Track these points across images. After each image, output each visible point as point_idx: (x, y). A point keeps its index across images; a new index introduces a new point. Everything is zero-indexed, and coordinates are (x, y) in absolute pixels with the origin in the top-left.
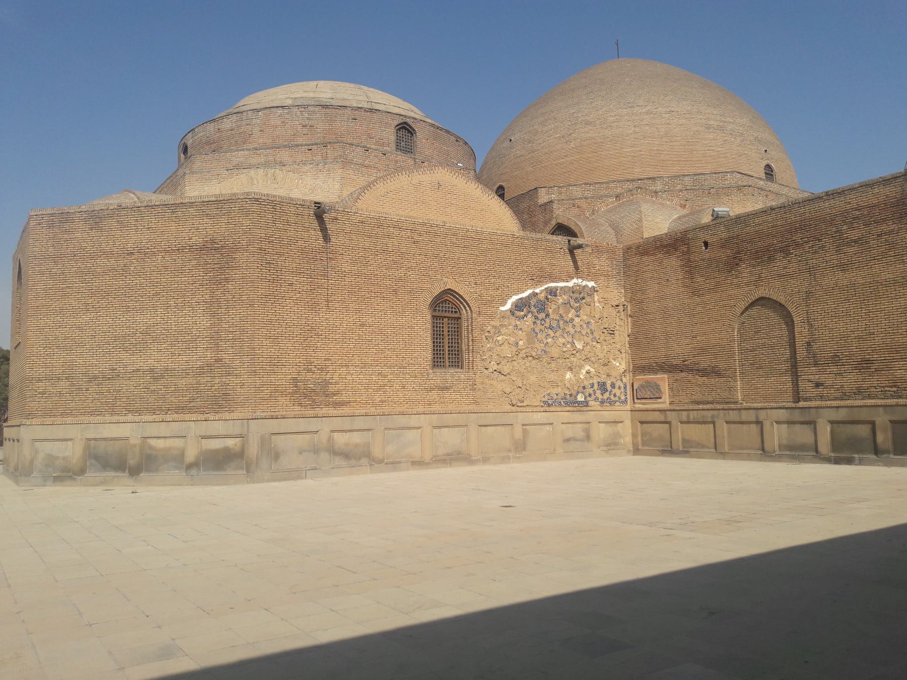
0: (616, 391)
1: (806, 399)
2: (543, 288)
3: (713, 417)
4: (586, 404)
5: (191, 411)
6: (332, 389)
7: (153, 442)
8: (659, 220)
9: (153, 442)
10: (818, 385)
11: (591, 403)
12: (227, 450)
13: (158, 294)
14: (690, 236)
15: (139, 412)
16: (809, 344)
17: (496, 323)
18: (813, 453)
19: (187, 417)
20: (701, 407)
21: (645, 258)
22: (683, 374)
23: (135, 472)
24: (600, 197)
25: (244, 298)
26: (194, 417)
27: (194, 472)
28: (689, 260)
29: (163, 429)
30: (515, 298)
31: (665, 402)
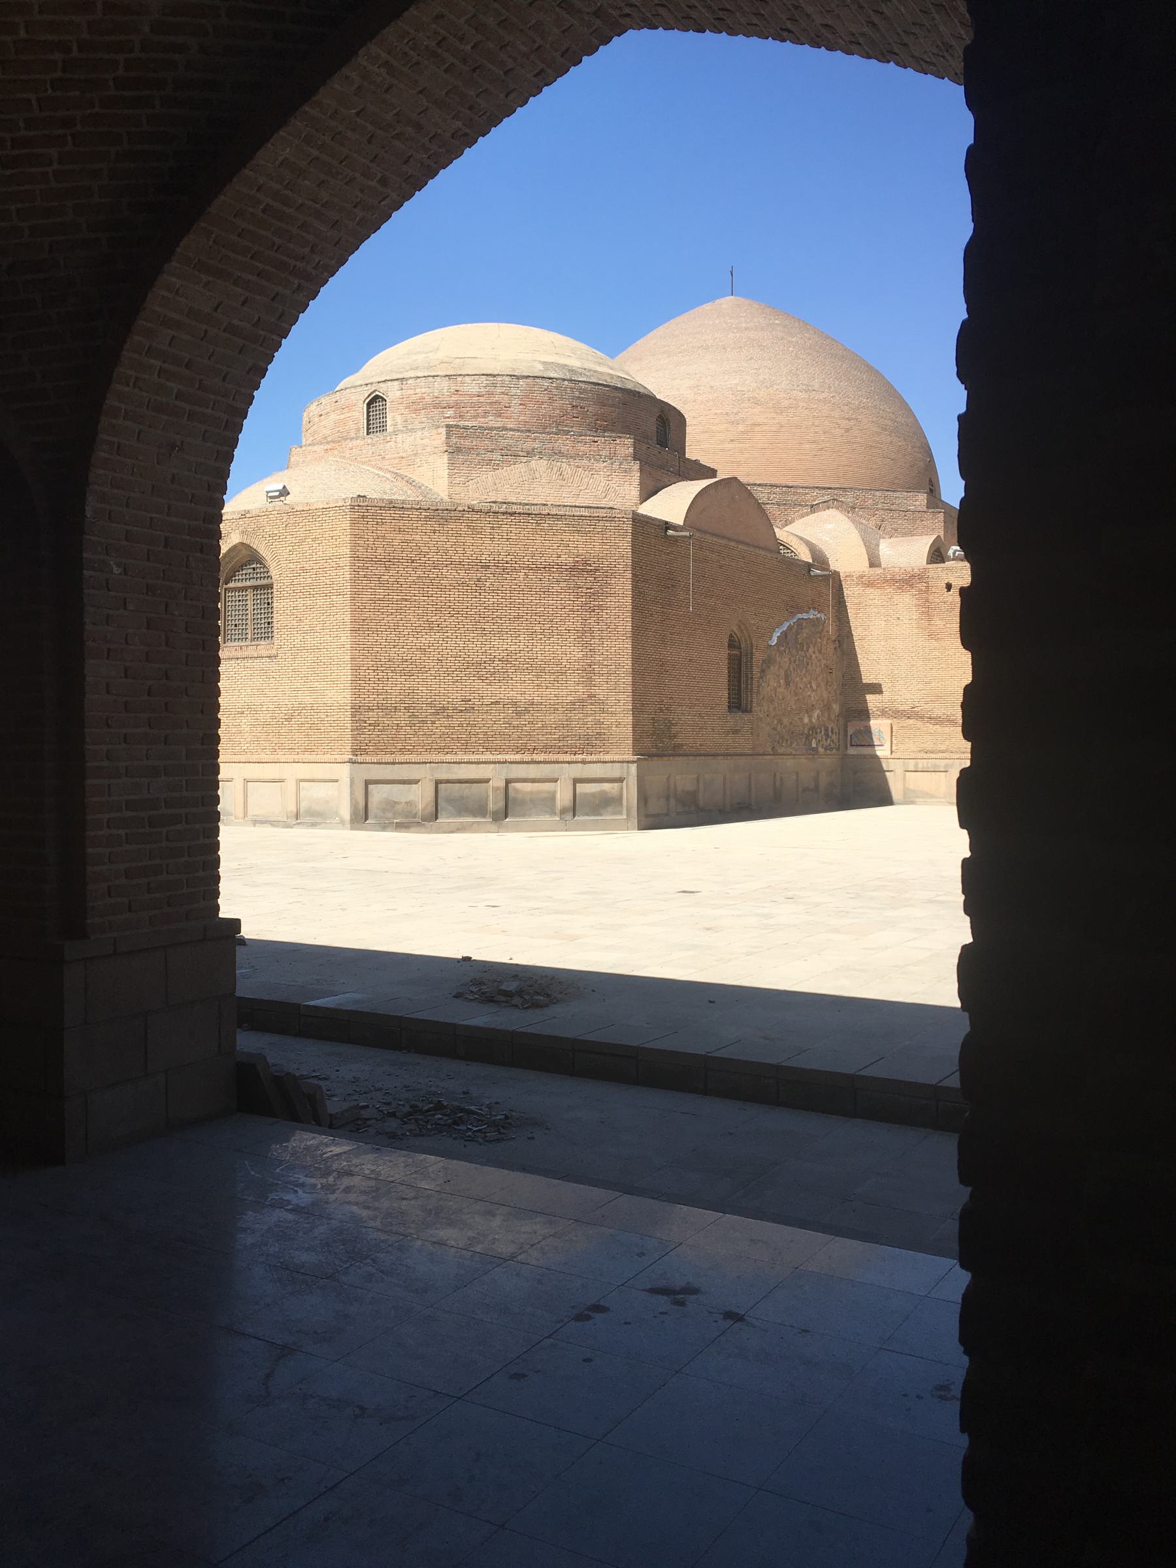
0: (834, 737)
3: (946, 766)
4: (815, 750)
6: (674, 730)
7: (518, 785)
11: (821, 750)
13: (519, 617)
14: (931, 574)
15: (500, 750)
19: (561, 757)
20: (933, 756)
21: (869, 590)
22: (911, 721)
25: (620, 629)
26: (568, 758)
27: (569, 816)
28: (927, 601)
29: (533, 771)
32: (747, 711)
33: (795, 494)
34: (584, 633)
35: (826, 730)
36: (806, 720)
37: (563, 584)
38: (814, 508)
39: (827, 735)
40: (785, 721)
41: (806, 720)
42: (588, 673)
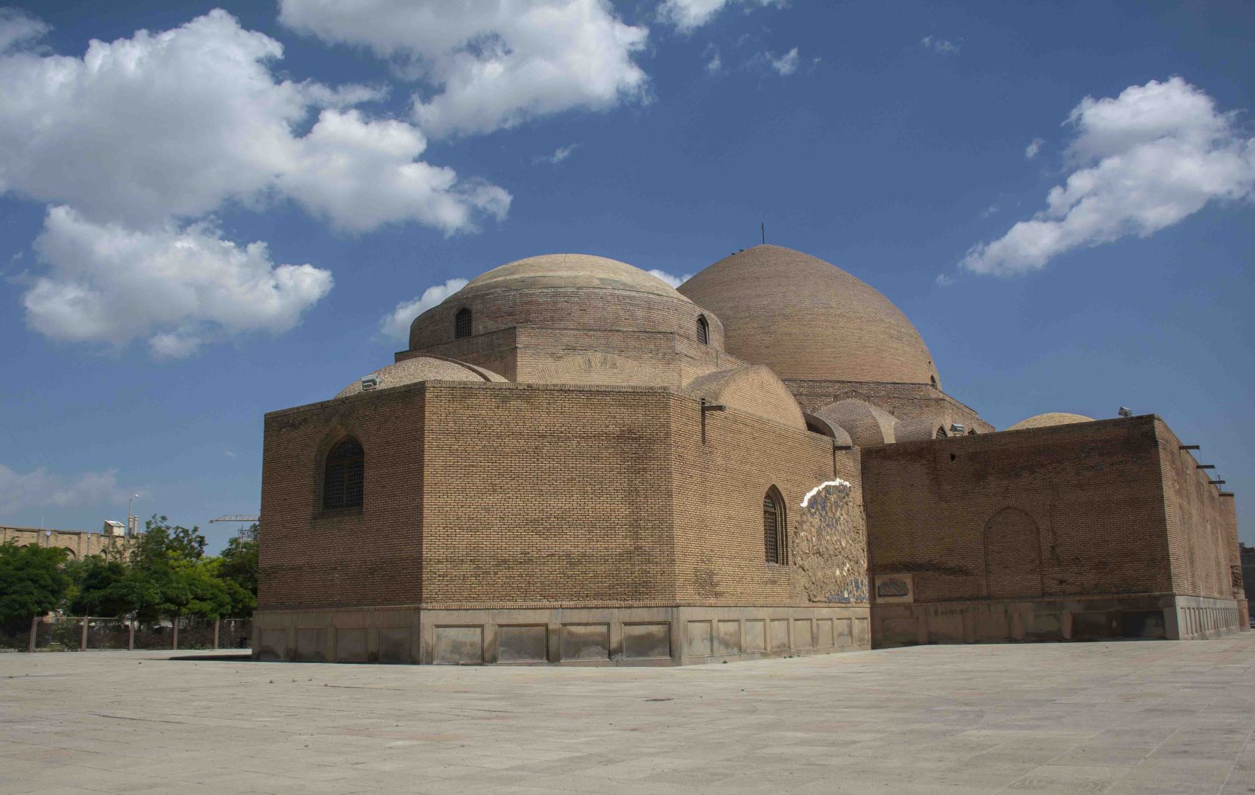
1: (1050, 595)
2: (823, 485)
5: (610, 597)
7: (573, 629)
8: (889, 429)
9: (573, 629)
10: (1061, 582)
12: (650, 636)
13: (573, 479)
16: (1053, 548)
17: (798, 519)
18: (1057, 637)
22: (930, 573)
23: (552, 658)
24: (819, 396)
25: (663, 488)
29: (583, 616)
30: (809, 496)
31: (909, 599)
32: (785, 562)
33: (820, 387)
34: (632, 492)
35: (857, 582)
36: (838, 573)
37: (611, 450)
38: (836, 398)
39: (857, 587)
40: (819, 574)
41: (838, 573)
42: (635, 527)
